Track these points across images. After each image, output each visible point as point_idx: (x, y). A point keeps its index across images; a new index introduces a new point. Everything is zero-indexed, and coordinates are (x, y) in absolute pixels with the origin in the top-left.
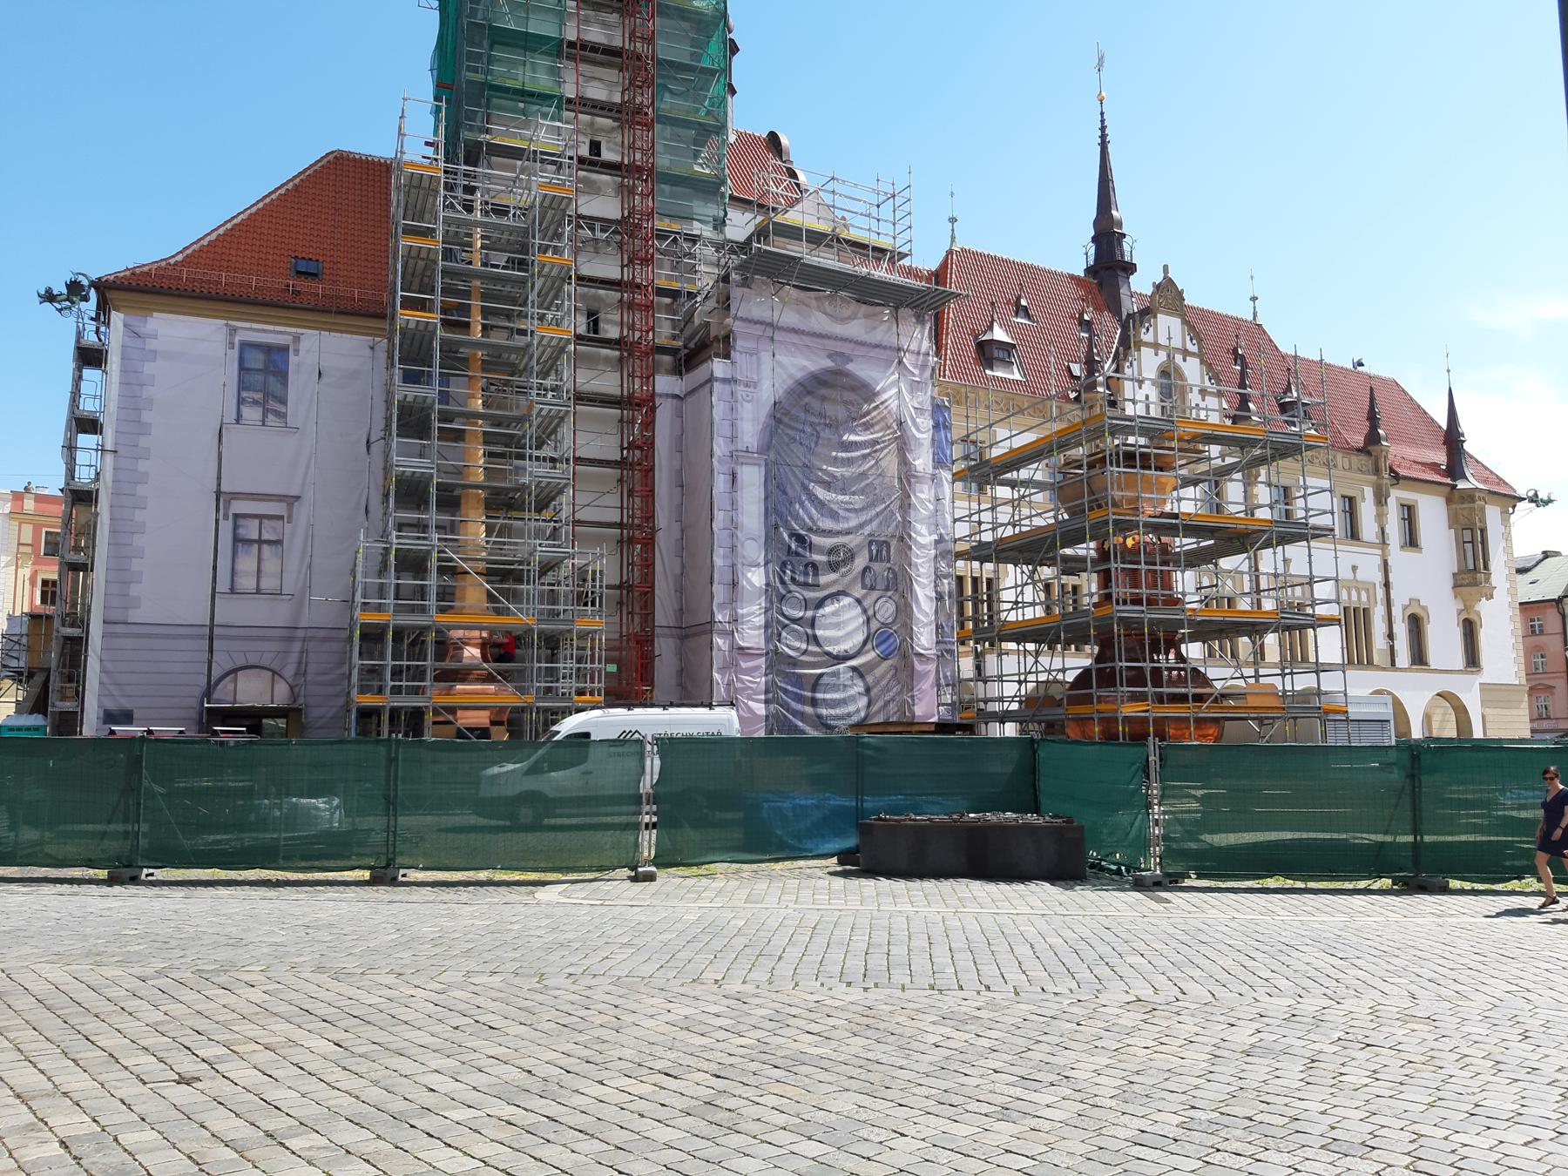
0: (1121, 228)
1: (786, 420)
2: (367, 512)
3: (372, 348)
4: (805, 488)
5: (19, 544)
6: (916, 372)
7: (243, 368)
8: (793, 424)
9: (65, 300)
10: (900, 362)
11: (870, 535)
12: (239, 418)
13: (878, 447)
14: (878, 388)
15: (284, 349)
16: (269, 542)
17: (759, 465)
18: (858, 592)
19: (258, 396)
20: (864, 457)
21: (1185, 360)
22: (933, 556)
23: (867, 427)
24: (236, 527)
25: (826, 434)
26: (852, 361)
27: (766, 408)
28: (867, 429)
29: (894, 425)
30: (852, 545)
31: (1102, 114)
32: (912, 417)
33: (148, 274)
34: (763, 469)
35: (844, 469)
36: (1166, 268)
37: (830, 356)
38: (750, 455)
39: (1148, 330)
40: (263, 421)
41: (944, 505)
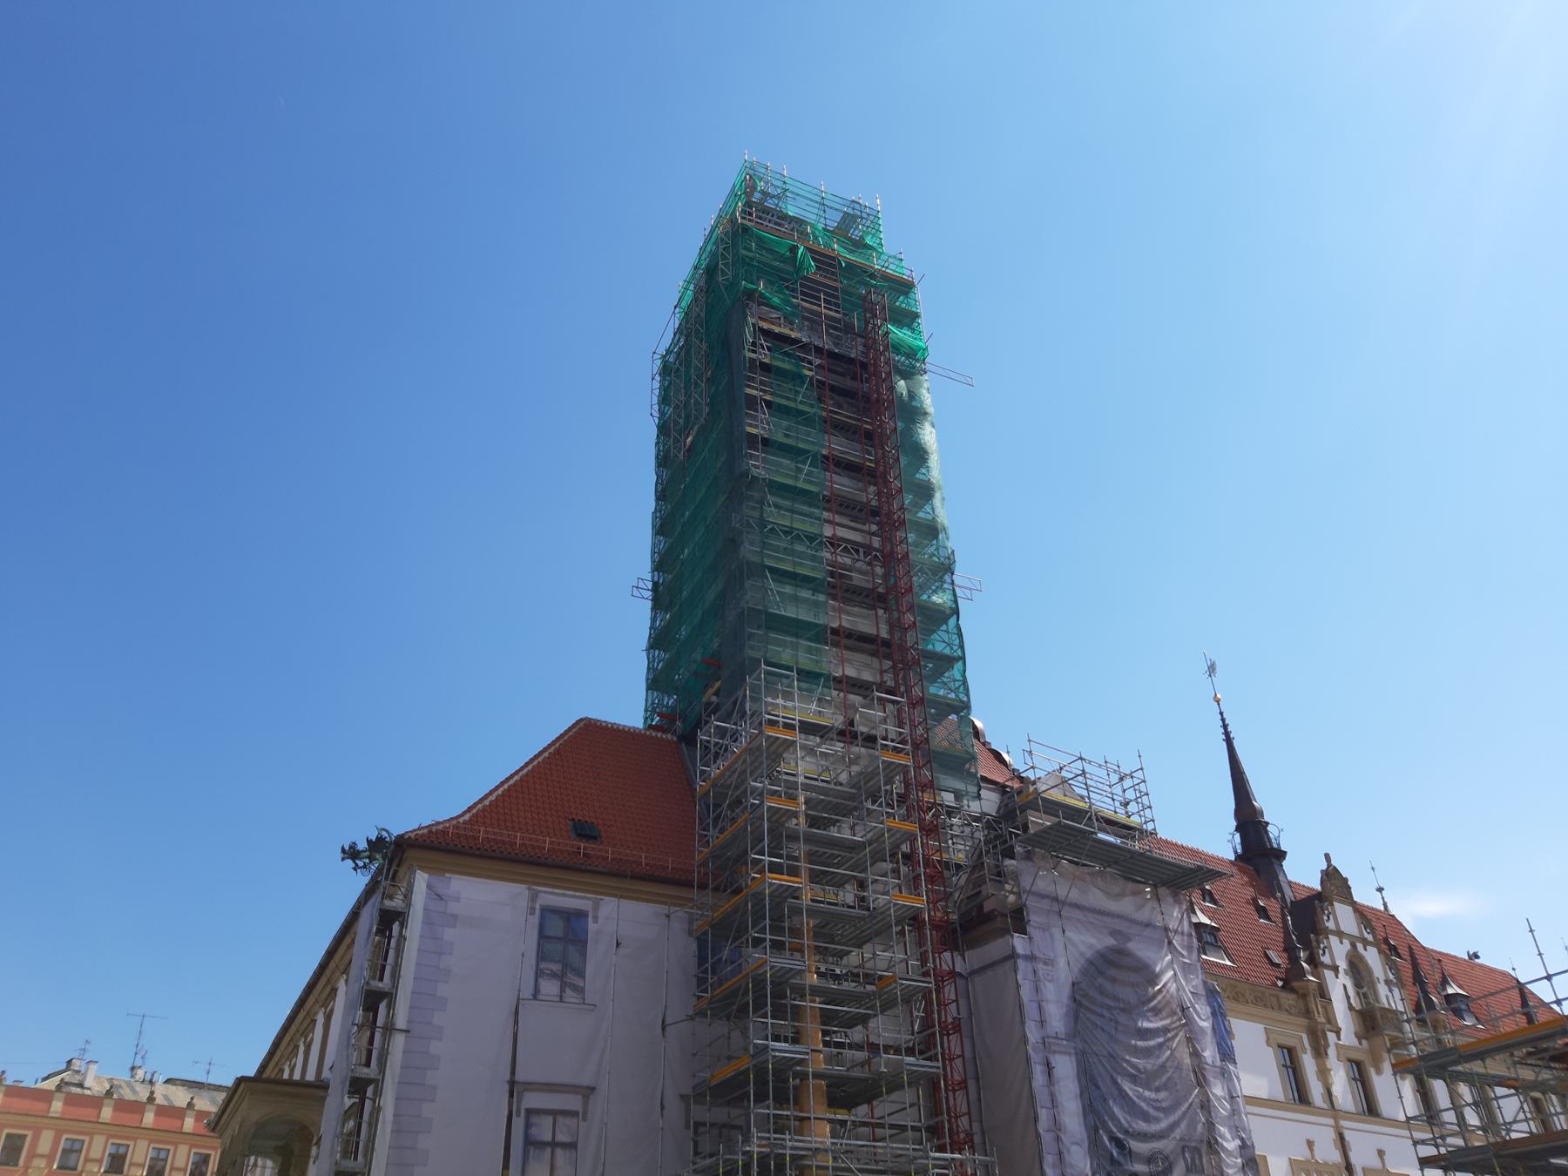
0: (1263, 817)
1: (1085, 1002)
2: (662, 1107)
3: (668, 916)
4: (1115, 1082)
6: (1185, 953)
7: (543, 936)
8: (1091, 1007)
9: (366, 858)
10: (1170, 943)
11: (1182, 1139)
12: (535, 995)
13: (1169, 1035)
14: (1158, 969)
15: (581, 915)
16: (564, 1145)
17: (1069, 1054)
19: (556, 967)
20: (1160, 1046)
21: (1365, 950)
22: (1241, 1164)
23: (1156, 1011)
24: (528, 1126)
25: (1122, 1019)
27: (1067, 990)
28: (1156, 1015)
29: (1178, 1010)
30: (1167, 1152)
32: (1191, 1002)
33: (444, 832)
34: (1074, 1058)
35: (1145, 1061)
36: (1327, 857)
38: (1060, 1042)
39: (1329, 917)
40: (561, 997)
41: (1238, 1103)
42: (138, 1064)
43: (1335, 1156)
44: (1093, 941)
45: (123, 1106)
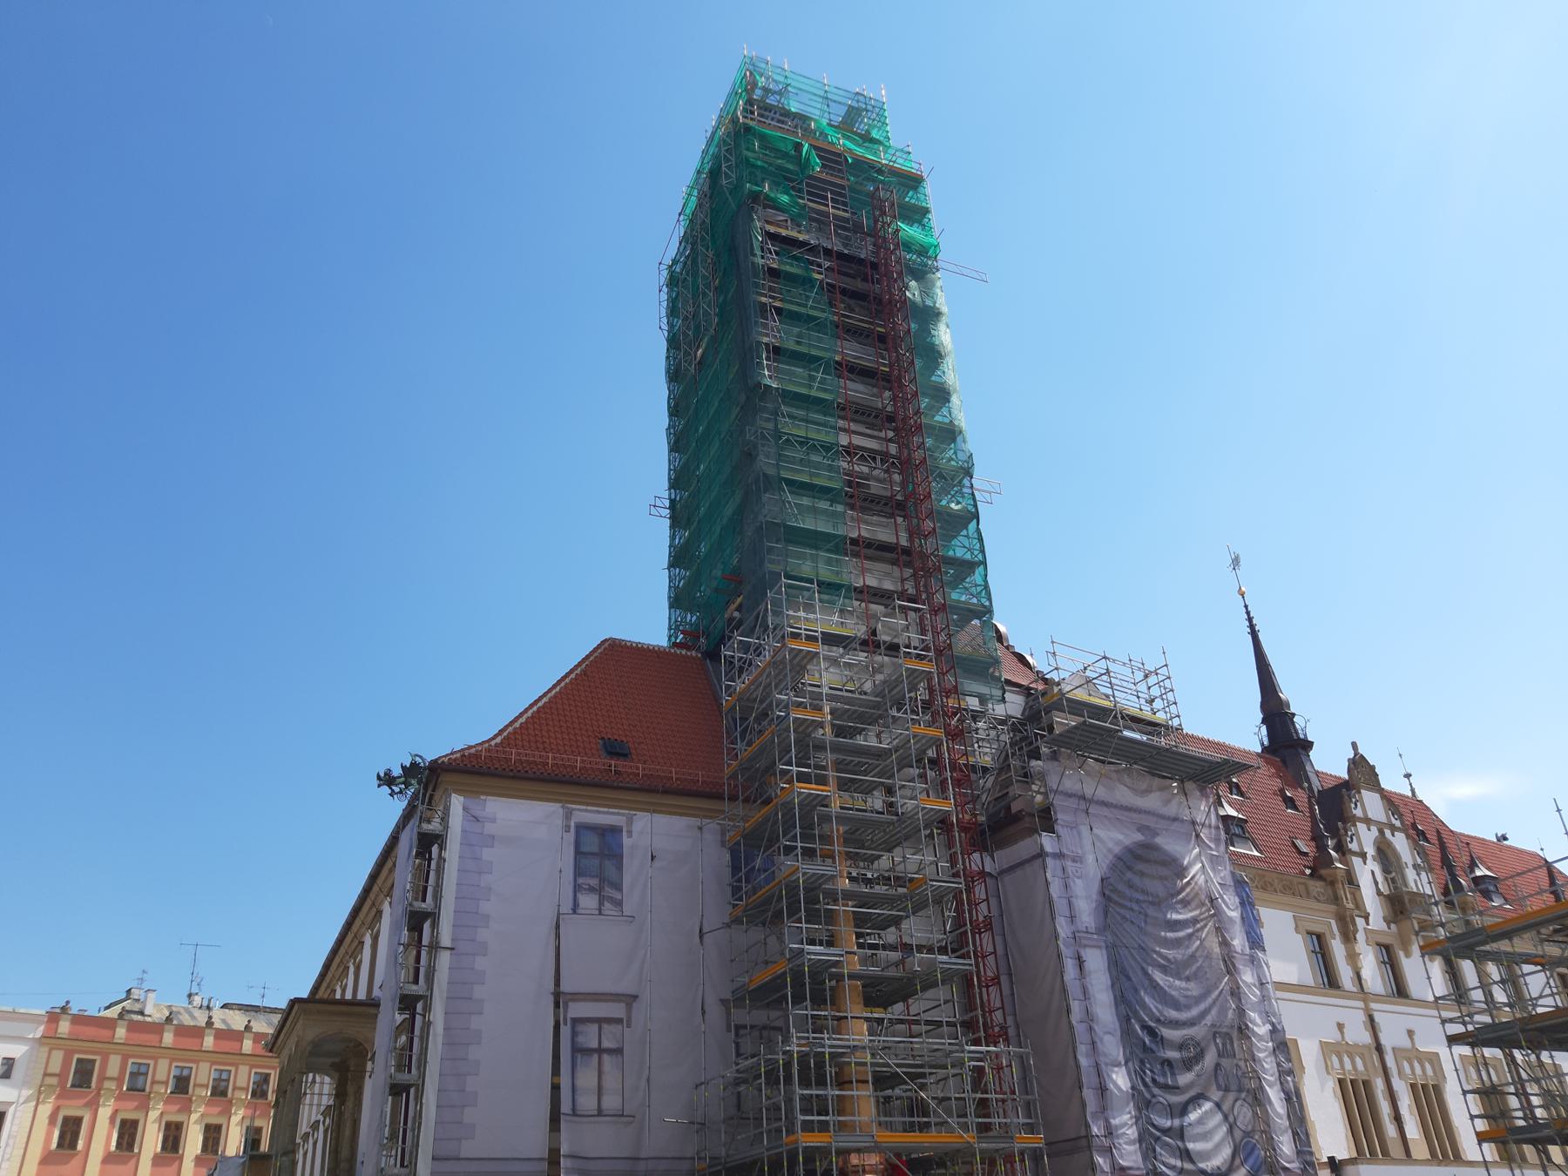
0: (1289, 708)
1: (1114, 897)
2: (704, 1013)
3: (700, 828)
4: (1146, 973)
5: (46, 1075)
6: (1213, 846)
7: (579, 853)
8: (1121, 901)
9: (402, 784)
10: (1198, 836)
11: (1213, 1025)
12: (575, 908)
13: (1198, 926)
14: (1185, 863)
15: (615, 831)
16: (610, 1051)
17: (1099, 947)
18: (1216, 1095)
19: (594, 882)
20: (1190, 936)
21: (1393, 835)
22: (1272, 1049)
23: (1185, 903)
24: (574, 1034)
25: (1151, 911)
26: (1158, 834)
27: (1096, 886)
28: (1185, 906)
29: (1207, 901)
30: (1198, 1038)
31: (1246, 607)
32: (1219, 893)
33: (477, 756)
34: (1104, 951)
35: (1175, 951)
36: (1354, 745)
37: (1139, 830)
38: (1090, 936)
39: (1356, 805)
40: (600, 910)
41: (1267, 989)
42: (193, 991)
43: (1366, 1038)
44: (1121, 837)
45: (182, 1031)
